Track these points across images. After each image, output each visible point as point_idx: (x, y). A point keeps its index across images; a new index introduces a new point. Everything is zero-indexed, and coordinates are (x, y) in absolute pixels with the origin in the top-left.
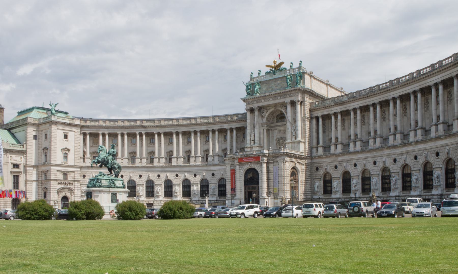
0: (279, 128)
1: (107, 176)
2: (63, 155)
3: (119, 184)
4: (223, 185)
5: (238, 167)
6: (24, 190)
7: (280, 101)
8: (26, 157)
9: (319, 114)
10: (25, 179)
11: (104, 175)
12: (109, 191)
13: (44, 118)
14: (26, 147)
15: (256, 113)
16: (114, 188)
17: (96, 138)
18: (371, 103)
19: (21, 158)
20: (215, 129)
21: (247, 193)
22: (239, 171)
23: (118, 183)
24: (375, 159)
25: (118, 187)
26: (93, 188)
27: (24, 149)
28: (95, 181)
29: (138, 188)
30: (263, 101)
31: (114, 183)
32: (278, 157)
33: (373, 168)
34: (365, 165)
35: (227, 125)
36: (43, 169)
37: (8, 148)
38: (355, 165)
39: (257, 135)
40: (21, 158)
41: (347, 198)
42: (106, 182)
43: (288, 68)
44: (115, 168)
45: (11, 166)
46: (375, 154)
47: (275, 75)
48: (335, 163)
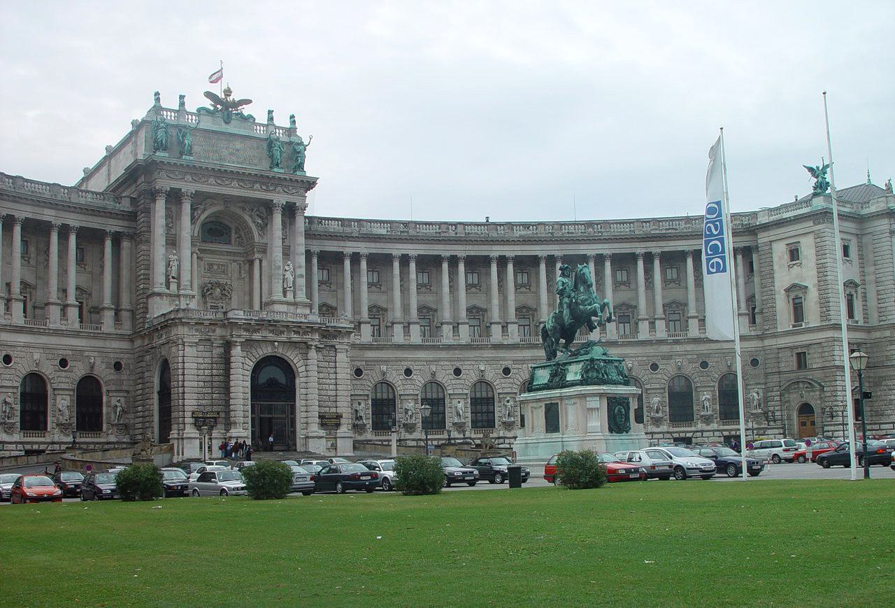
0: (208, 258)
4: (488, 399)
5: (237, 351)
7: (258, 194)
9: (316, 247)
15: (187, 207)
18: (448, 254)
20: (17, 215)
21: (257, 422)
22: (241, 360)
24: (458, 364)
30: (212, 180)
32: (335, 337)
33: (453, 382)
34: (434, 374)
35: (52, 212)
38: (408, 372)
39: (186, 265)
41: (438, 440)
43: (262, 118)
46: (458, 354)
47: (227, 123)
48: (358, 364)
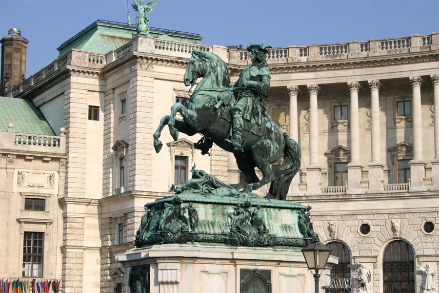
1: (226, 191)
2: (173, 163)
3: (286, 227)
6: (59, 277)
8: (67, 173)
10: (61, 244)
11: (213, 184)
12: (233, 261)
13: (118, 51)
14: (67, 143)
16: (259, 244)
17: (280, 105)
19: (51, 177)
23: (281, 222)
25: (275, 243)
26: (155, 247)
27: (61, 150)
28: (168, 212)
29: (420, 267)
31: (257, 223)
36: (116, 209)
37: (12, 146)
40: (51, 177)
42: (219, 219)
44: (265, 150)
45: (20, 203)
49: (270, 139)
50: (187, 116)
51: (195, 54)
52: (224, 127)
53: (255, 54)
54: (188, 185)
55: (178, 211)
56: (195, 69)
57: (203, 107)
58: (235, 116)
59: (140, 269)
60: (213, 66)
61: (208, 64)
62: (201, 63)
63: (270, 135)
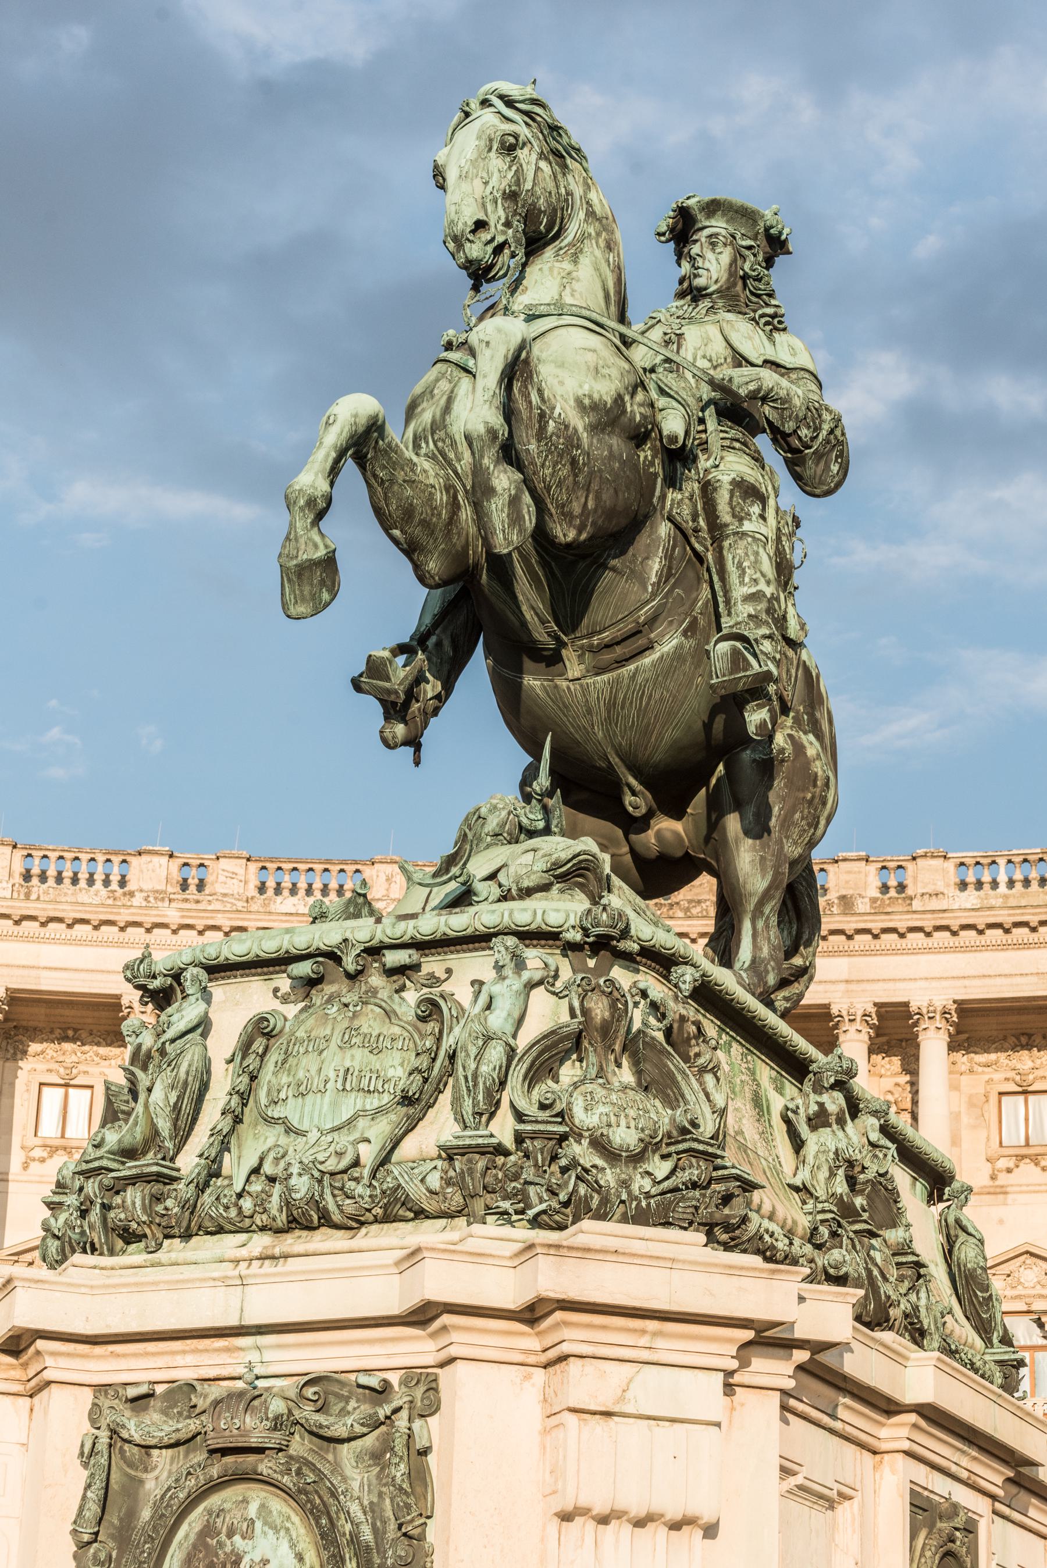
49: (819, 737)
50: (551, 422)
51: (509, 103)
52: (667, 574)
53: (726, 256)
54: (557, 865)
55: (600, 1009)
56: (518, 183)
57: (615, 401)
58: (747, 526)
59: (277, 1406)
60: (598, 209)
61: (578, 191)
62: (543, 164)
63: (818, 715)
